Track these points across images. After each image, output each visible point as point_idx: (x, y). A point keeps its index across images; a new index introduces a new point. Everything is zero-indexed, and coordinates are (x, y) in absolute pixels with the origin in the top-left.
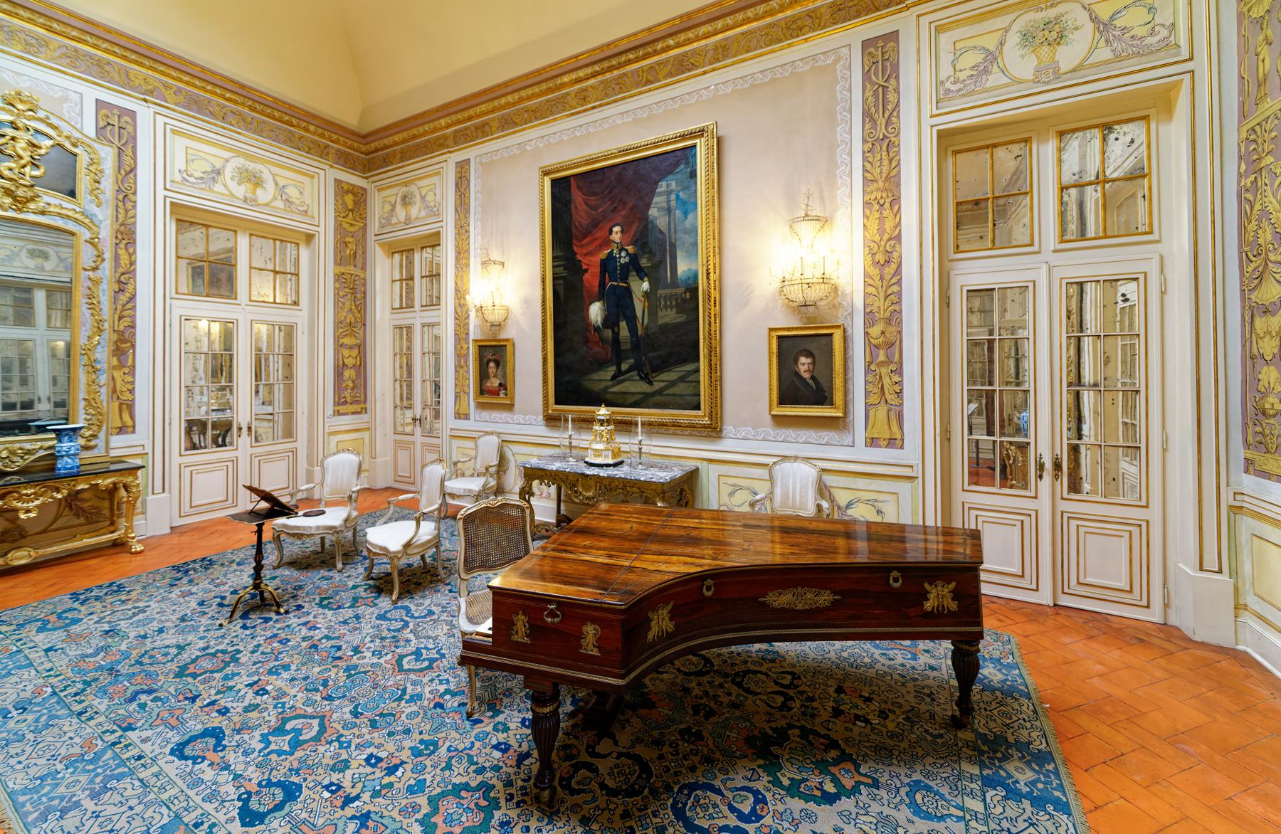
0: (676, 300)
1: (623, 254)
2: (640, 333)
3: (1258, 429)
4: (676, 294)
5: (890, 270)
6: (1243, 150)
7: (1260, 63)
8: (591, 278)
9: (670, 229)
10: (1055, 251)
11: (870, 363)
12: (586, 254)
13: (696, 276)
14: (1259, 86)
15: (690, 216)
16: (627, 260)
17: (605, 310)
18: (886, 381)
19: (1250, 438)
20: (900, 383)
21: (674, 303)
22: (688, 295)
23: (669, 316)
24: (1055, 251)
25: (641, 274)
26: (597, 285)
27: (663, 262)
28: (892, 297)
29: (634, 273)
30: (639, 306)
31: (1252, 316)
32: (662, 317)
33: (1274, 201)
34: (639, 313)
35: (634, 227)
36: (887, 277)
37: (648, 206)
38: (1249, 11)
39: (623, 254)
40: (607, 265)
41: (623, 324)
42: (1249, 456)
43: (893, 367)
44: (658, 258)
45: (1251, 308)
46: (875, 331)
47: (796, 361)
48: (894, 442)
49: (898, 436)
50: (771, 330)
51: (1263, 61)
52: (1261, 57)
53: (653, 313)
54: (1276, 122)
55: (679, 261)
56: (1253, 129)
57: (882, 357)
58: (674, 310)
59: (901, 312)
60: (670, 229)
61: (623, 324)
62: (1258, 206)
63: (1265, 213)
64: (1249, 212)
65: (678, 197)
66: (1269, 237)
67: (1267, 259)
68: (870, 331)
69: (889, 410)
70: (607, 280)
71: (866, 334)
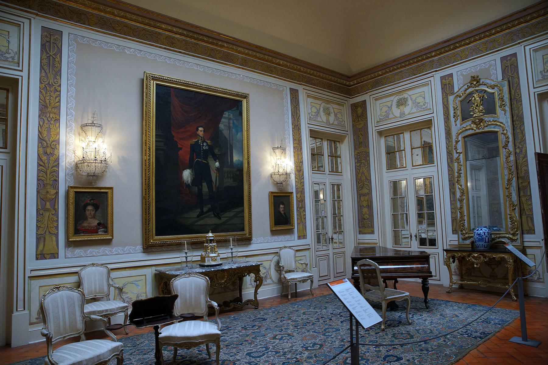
1: (205, 144)
2: (214, 190)
5: (301, 173)
8: (184, 154)
9: (230, 137)
13: (242, 164)
14: (360, 144)
15: (239, 134)
16: (207, 148)
18: (302, 214)
19: (360, 226)
20: (305, 215)
21: (232, 176)
23: (229, 182)
25: (216, 158)
26: (188, 159)
29: (211, 156)
34: (214, 179)
37: (219, 122)
39: (205, 144)
40: (195, 148)
41: (204, 184)
42: (360, 230)
43: (303, 209)
45: (360, 195)
46: (299, 195)
47: (279, 206)
48: (304, 237)
49: (305, 235)
50: (272, 193)
51: (361, 138)
52: (360, 137)
55: (234, 155)
56: (358, 153)
57: (300, 206)
58: (232, 180)
59: (304, 189)
60: (230, 137)
61: (204, 184)
62: (361, 171)
63: (363, 173)
65: (233, 123)
68: (297, 195)
69: (303, 225)
70: (195, 157)
71: (296, 196)
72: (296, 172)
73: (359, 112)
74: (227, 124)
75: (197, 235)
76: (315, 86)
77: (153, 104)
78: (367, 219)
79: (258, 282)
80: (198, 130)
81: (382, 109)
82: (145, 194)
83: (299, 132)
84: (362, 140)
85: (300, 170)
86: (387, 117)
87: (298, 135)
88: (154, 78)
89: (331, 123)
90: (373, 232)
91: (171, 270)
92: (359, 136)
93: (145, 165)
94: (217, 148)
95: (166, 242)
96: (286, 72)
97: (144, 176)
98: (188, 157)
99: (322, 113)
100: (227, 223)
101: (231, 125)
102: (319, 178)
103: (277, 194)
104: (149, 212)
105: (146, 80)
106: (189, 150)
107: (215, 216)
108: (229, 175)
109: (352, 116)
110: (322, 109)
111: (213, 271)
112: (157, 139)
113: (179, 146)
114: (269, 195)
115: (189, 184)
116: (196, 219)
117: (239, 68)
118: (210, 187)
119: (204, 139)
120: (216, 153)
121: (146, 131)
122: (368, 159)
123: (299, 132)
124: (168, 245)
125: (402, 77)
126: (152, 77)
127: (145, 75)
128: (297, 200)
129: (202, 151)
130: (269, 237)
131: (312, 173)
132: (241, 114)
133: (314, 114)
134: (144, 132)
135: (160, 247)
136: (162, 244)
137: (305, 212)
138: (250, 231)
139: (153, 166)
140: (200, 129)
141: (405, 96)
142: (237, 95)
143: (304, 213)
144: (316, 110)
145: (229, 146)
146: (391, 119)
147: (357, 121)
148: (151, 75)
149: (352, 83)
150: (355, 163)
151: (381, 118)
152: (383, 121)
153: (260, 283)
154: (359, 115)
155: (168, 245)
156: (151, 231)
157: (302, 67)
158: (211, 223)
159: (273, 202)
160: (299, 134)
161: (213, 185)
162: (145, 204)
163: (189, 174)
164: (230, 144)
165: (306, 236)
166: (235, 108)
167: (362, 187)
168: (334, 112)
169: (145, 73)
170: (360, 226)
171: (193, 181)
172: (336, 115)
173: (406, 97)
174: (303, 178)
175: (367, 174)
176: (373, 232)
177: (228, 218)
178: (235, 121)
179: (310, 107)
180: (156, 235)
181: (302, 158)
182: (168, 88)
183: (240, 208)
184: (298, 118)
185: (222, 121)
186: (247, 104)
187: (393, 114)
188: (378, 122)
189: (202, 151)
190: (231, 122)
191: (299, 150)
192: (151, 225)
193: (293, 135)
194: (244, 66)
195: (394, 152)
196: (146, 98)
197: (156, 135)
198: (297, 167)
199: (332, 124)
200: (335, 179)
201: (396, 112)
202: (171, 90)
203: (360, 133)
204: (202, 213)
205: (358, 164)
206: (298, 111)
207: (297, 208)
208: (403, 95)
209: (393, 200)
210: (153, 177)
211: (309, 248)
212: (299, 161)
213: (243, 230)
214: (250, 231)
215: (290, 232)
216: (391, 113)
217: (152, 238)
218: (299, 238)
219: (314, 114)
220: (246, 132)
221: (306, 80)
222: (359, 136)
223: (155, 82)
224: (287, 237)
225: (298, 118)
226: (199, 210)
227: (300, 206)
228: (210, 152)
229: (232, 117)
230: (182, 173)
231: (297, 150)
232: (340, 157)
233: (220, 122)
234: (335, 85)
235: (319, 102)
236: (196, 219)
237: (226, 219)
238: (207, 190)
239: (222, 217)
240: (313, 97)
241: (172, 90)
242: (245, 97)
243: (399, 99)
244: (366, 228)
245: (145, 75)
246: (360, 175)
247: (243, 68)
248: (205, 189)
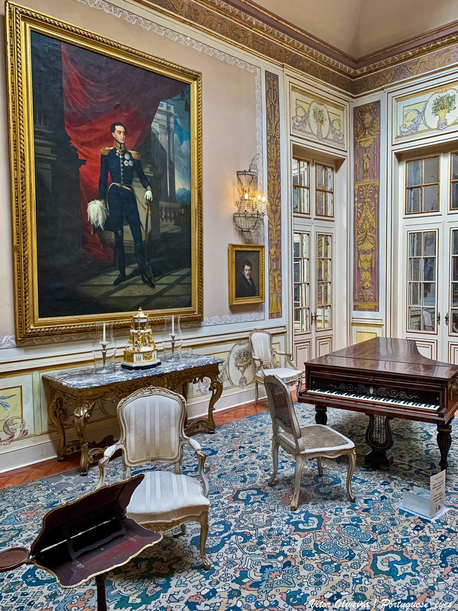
0: (175, 214)
1: (127, 157)
2: (144, 239)
3: (360, 294)
4: (174, 208)
6: (356, 192)
7: (365, 164)
10: (315, 219)
11: (271, 269)
12: (83, 144)
13: (189, 195)
14: (364, 172)
15: (185, 143)
16: (131, 163)
17: (106, 211)
18: (276, 280)
19: (356, 298)
20: (280, 281)
21: (172, 215)
22: (183, 210)
24: (315, 219)
25: (145, 183)
26: (97, 181)
27: (164, 175)
28: (278, 231)
29: (138, 179)
30: (143, 213)
31: (359, 254)
32: (163, 227)
33: (371, 215)
34: (143, 220)
35: (138, 133)
36: (276, 220)
37: (151, 119)
38: (360, 142)
39: (127, 157)
41: (127, 228)
42: (355, 304)
43: (278, 272)
44: (159, 171)
46: (273, 251)
47: (243, 267)
50: (234, 246)
51: (366, 164)
52: (365, 162)
53: (155, 222)
54: (372, 188)
55: (176, 179)
56: (361, 186)
57: (275, 267)
58: (173, 221)
59: (281, 241)
61: (127, 228)
62: (363, 215)
63: (366, 218)
64: (359, 216)
65: (176, 123)
66: (368, 227)
67: (366, 235)
68: (271, 250)
69: (277, 297)
71: (269, 252)
72: (271, 214)
73: (366, 121)
74: (165, 124)
75: (115, 314)
76: (304, 71)
77: (27, 70)
78: (368, 289)
79: (215, 390)
80: (115, 129)
81: (406, 116)
82: (18, 243)
83: (277, 148)
84: (368, 167)
85: (276, 211)
86: (415, 129)
87: (275, 152)
88: (27, 17)
89: (324, 136)
90: (376, 309)
91: (71, 376)
92: (364, 160)
93: (16, 189)
94: (149, 165)
95: (58, 327)
96: (260, 42)
97: (14, 209)
99: (312, 119)
100: (164, 295)
101: (172, 126)
102: (300, 224)
103: (241, 248)
104: (25, 275)
105: (10, 18)
106: (99, 165)
107: (145, 282)
108: (168, 215)
109: (355, 126)
110: (312, 113)
111: (146, 377)
112: (38, 141)
113: (81, 157)
114: (229, 250)
115: (99, 227)
116: (113, 288)
117: (184, 22)
119: (125, 147)
120: (145, 174)
121: (14, 122)
122: (376, 196)
123: (277, 148)
124: (63, 333)
125: (449, 60)
126: (23, 13)
127: (7, 7)
128: (270, 258)
129: (122, 170)
130: (228, 316)
131: (294, 216)
132: (188, 108)
133: (299, 119)
134: (12, 124)
135: (47, 337)
136: (52, 331)
137: (281, 277)
138: (200, 307)
139: (31, 191)
140: (119, 128)
141: (451, 92)
142: (183, 72)
143: (280, 279)
144: (303, 114)
145: (168, 164)
146: (421, 132)
147: (362, 136)
148: (19, 9)
149: (358, 72)
150: (355, 202)
151: (405, 130)
152: (408, 135)
153: (219, 390)
154: (366, 126)
155: (63, 333)
156: (31, 309)
157: (287, 34)
158: (138, 294)
159: (234, 261)
160: (277, 151)
161: (142, 232)
162: (19, 261)
163: (100, 209)
165: (280, 314)
166: (179, 97)
167: (364, 240)
168: (329, 119)
169: (7, 4)
170: (356, 298)
171: (107, 222)
172: (331, 124)
173: (451, 95)
174: (280, 224)
175: (373, 220)
176: (376, 309)
177: (166, 286)
178: (178, 120)
179: (294, 107)
180: (40, 316)
181: (280, 191)
182: (56, 42)
183: (185, 269)
184: (277, 124)
185: (155, 116)
186: (198, 91)
187: (425, 124)
188: (398, 137)
189: (122, 170)
190: (172, 120)
191: (276, 177)
192: (30, 297)
193: (268, 152)
194: (193, 20)
195: (420, 187)
196: (12, 55)
197: (35, 132)
198: (272, 205)
199: (325, 138)
200: (323, 227)
201: (432, 121)
202: (62, 47)
203: (365, 155)
204: (123, 277)
205: (359, 205)
206: (276, 112)
207: (270, 270)
208: (446, 91)
209: (425, 260)
210: (31, 210)
211: (285, 331)
212: (276, 196)
213: (189, 304)
214: (200, 307)
215: (257, 307)
216: (422, 122)
217: (32, 320)
218: (271, 316)
219: (299, 119)
220: (196, 141)
221: (291, 59)
222: (364, 160)
223: (28, 25)
224: (254, 315)
225: (277, 124)
226: (118, 272)
227: (275, 267)
229: (173, 112)
230: (87, 207)
231: (272, 177)
232: (332, 193)
233: (153, 118)
234: (333, 74)
235: (309, 100)
236: (113, 288)
237: (163, 287)
238: (132, 239)
239: (157, 284)
240: (300, 90)
241: (63, 46)
242: (196, 77)
243: (438, 98)
244: (364, 301)
245: (7, 7)
246: (361, 221)
247: (191, 24)
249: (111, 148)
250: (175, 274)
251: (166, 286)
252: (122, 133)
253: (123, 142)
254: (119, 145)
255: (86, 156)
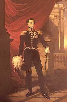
1: (35, 33)
8: (15, 44)
16: (37, 37)
21: (63, 60)
25: (45, 45)
30: (43, 60)
40: (26, 38)
70: (25, 45)
98: (18, 46)
118: (39, 70)
164: (61, 32)
189: (32, 40)
228: (41, 39)
248: (34, 70)
249: (27, 31)
250: (63, 91)
251: (57, 99)
252: (32, 23)
253: (33, 27)
254: (31, 29)
255: (13, 37)
